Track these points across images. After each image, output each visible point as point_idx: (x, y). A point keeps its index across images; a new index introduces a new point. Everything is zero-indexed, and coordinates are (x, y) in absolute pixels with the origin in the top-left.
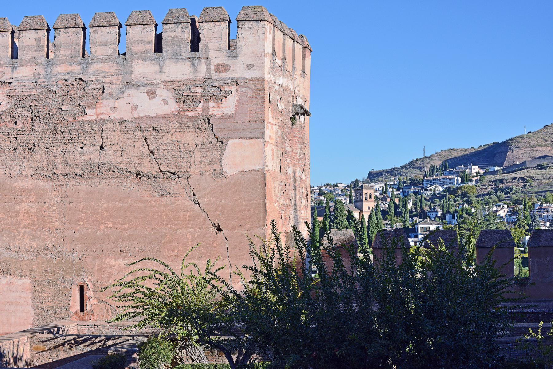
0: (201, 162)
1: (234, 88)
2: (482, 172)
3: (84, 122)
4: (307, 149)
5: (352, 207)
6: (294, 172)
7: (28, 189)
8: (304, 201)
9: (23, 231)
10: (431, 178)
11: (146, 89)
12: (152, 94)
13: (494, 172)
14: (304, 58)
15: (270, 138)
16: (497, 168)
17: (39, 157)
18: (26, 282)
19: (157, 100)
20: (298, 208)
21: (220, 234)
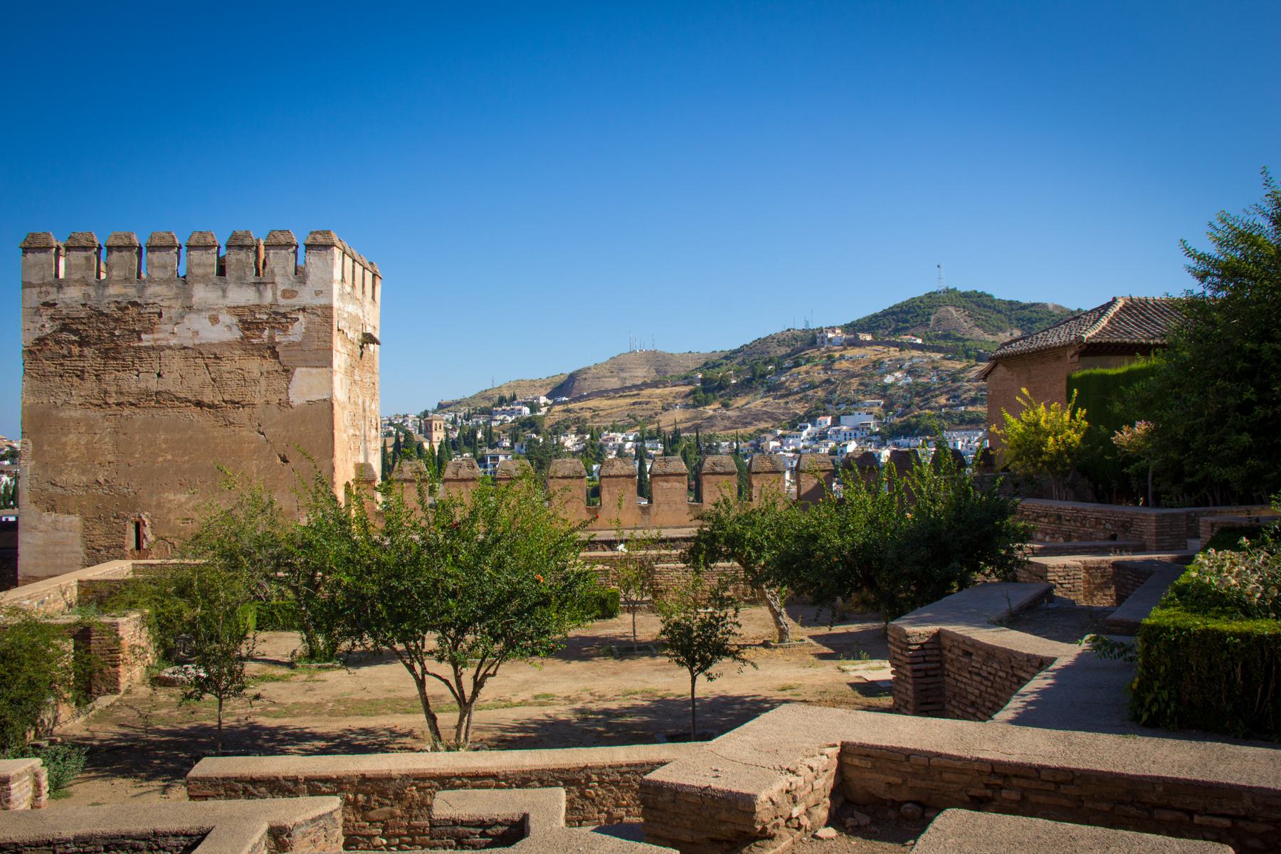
0: (266, 391)
1: (301, 316)
2: (550, 402)
3: (140, 348)
4: (377, 378)
5: (421, 438)
6: (364, 403)
7: (77, 419)
8: (373, 431)
9: (71, 464)
10: (508, 408)
11: (207, 315)
12: (214, 320)
13: (564, 403)
14: (374, 287)
15: (339, 366)
16: (564, 399)
17: (90, 384)
18: (76, 520)
19: (218, 327)
20: (367, 438)
21: (287, 467)
